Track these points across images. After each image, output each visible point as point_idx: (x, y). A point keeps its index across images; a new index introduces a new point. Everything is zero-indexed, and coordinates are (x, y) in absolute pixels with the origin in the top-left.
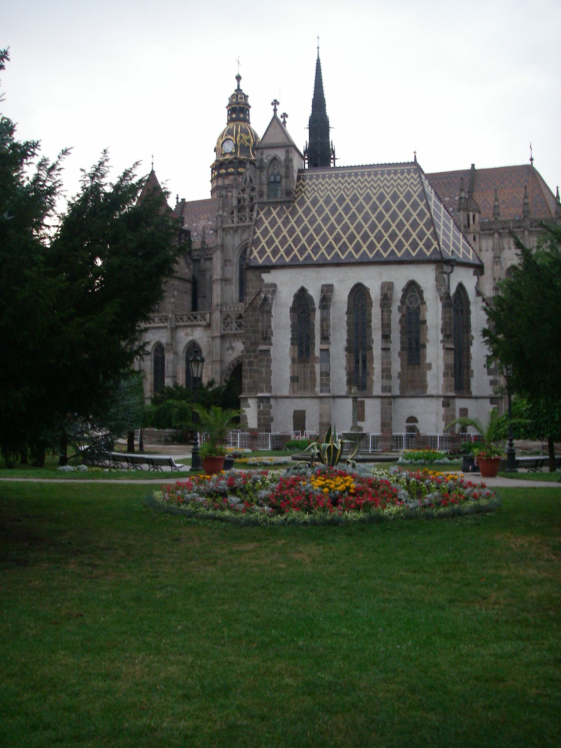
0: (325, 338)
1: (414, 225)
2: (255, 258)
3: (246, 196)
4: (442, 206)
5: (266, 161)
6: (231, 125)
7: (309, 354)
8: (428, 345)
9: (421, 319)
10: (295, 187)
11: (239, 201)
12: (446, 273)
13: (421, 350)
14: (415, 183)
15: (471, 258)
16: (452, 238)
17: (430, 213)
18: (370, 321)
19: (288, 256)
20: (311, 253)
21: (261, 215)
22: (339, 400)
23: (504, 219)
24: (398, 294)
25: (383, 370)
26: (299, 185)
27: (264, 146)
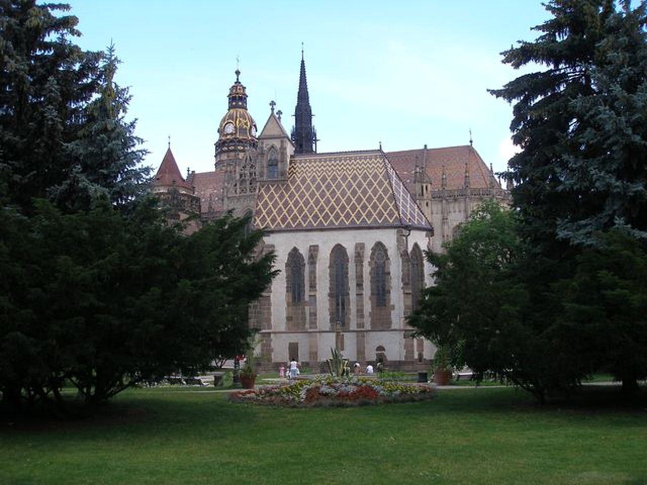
0: (313, 287)
1: (380, 199)
2: (258, 225)
3: (247, 172)
4: (401, 184)
5: (265, 149)
6: (232, 111)
7: (300, 299)
8: (391, 291)
9: (386, 271)
10: (288, 170)
11: (241, 175)
12: (404, 236)
13: (387, 295)
14: (381, 166)
15: (423, 223)
16: (409, 209)
17: (392, 190)
18: (347, 273)
19: (283, 224)
20: (301, 221)
21: (262, 191)
22: (324, 334)
23: (450, 189)
24: (368, 252)
25: (358, 311)
27: (263, 137)
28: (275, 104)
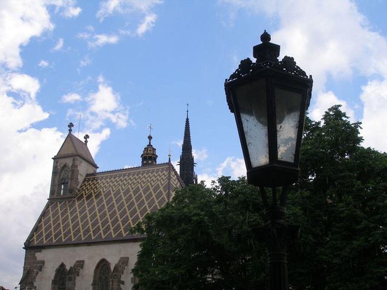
5: (59, 168)
27: (59, 157)
28: (73, 126)
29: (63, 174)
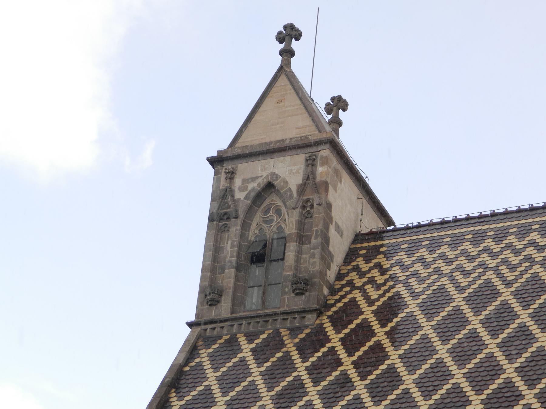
5: (240, 195)
26: (350, 271)
28: (298, 36)
29: (257, 219)
